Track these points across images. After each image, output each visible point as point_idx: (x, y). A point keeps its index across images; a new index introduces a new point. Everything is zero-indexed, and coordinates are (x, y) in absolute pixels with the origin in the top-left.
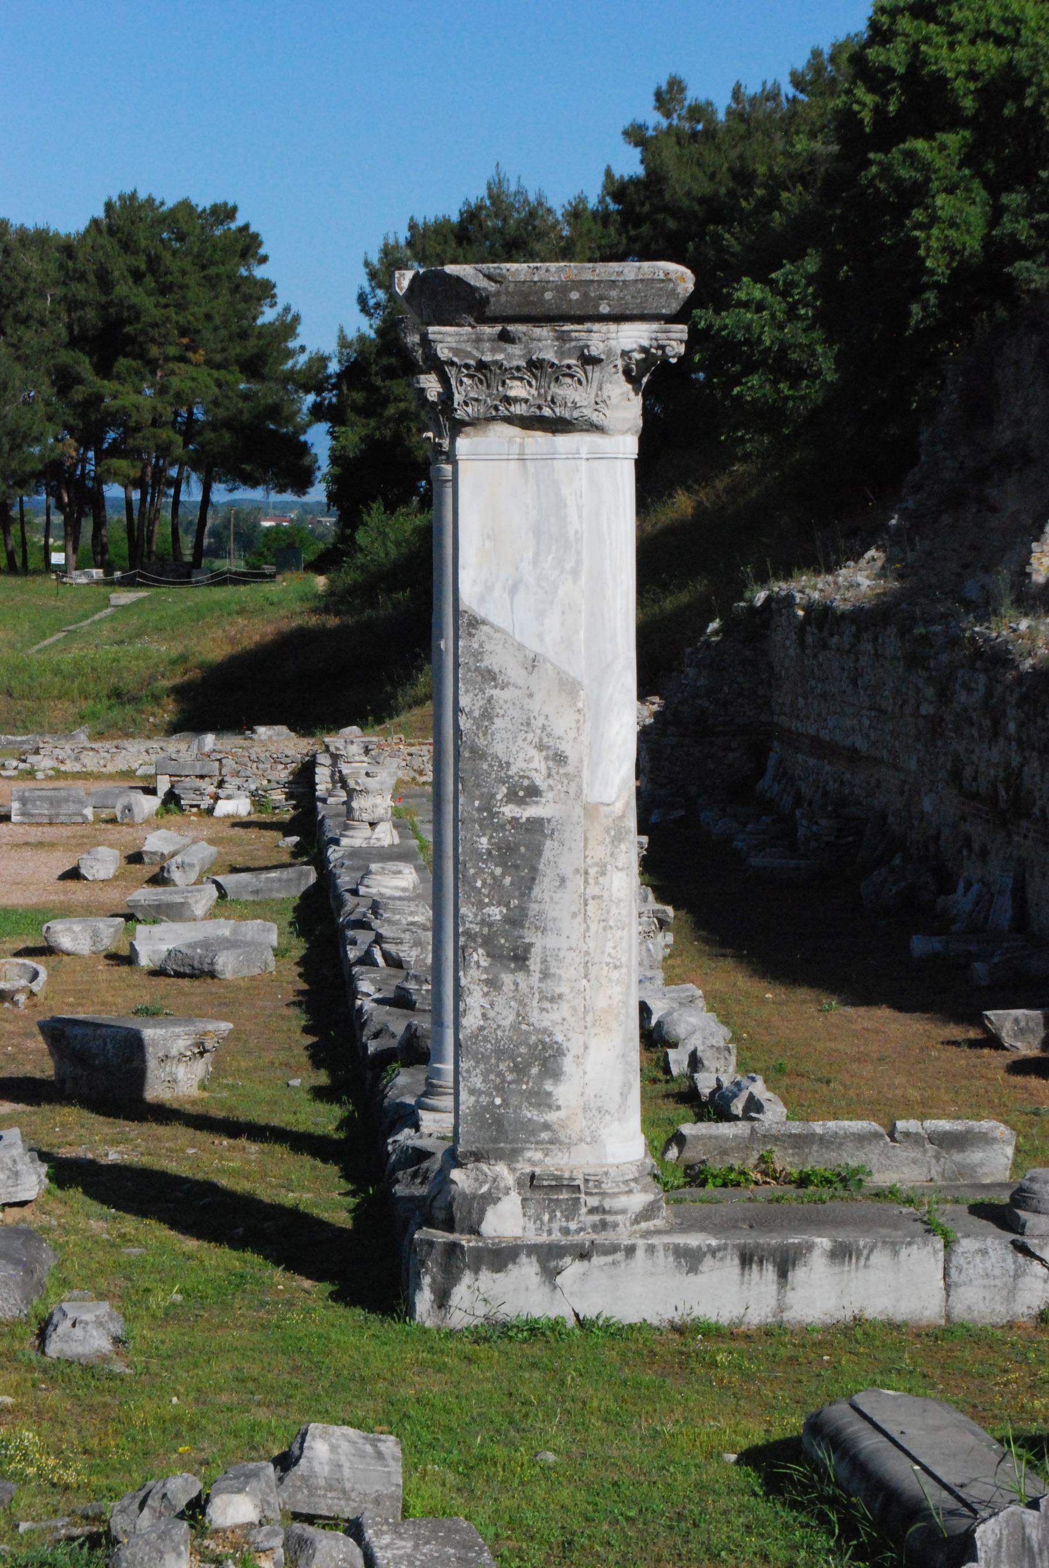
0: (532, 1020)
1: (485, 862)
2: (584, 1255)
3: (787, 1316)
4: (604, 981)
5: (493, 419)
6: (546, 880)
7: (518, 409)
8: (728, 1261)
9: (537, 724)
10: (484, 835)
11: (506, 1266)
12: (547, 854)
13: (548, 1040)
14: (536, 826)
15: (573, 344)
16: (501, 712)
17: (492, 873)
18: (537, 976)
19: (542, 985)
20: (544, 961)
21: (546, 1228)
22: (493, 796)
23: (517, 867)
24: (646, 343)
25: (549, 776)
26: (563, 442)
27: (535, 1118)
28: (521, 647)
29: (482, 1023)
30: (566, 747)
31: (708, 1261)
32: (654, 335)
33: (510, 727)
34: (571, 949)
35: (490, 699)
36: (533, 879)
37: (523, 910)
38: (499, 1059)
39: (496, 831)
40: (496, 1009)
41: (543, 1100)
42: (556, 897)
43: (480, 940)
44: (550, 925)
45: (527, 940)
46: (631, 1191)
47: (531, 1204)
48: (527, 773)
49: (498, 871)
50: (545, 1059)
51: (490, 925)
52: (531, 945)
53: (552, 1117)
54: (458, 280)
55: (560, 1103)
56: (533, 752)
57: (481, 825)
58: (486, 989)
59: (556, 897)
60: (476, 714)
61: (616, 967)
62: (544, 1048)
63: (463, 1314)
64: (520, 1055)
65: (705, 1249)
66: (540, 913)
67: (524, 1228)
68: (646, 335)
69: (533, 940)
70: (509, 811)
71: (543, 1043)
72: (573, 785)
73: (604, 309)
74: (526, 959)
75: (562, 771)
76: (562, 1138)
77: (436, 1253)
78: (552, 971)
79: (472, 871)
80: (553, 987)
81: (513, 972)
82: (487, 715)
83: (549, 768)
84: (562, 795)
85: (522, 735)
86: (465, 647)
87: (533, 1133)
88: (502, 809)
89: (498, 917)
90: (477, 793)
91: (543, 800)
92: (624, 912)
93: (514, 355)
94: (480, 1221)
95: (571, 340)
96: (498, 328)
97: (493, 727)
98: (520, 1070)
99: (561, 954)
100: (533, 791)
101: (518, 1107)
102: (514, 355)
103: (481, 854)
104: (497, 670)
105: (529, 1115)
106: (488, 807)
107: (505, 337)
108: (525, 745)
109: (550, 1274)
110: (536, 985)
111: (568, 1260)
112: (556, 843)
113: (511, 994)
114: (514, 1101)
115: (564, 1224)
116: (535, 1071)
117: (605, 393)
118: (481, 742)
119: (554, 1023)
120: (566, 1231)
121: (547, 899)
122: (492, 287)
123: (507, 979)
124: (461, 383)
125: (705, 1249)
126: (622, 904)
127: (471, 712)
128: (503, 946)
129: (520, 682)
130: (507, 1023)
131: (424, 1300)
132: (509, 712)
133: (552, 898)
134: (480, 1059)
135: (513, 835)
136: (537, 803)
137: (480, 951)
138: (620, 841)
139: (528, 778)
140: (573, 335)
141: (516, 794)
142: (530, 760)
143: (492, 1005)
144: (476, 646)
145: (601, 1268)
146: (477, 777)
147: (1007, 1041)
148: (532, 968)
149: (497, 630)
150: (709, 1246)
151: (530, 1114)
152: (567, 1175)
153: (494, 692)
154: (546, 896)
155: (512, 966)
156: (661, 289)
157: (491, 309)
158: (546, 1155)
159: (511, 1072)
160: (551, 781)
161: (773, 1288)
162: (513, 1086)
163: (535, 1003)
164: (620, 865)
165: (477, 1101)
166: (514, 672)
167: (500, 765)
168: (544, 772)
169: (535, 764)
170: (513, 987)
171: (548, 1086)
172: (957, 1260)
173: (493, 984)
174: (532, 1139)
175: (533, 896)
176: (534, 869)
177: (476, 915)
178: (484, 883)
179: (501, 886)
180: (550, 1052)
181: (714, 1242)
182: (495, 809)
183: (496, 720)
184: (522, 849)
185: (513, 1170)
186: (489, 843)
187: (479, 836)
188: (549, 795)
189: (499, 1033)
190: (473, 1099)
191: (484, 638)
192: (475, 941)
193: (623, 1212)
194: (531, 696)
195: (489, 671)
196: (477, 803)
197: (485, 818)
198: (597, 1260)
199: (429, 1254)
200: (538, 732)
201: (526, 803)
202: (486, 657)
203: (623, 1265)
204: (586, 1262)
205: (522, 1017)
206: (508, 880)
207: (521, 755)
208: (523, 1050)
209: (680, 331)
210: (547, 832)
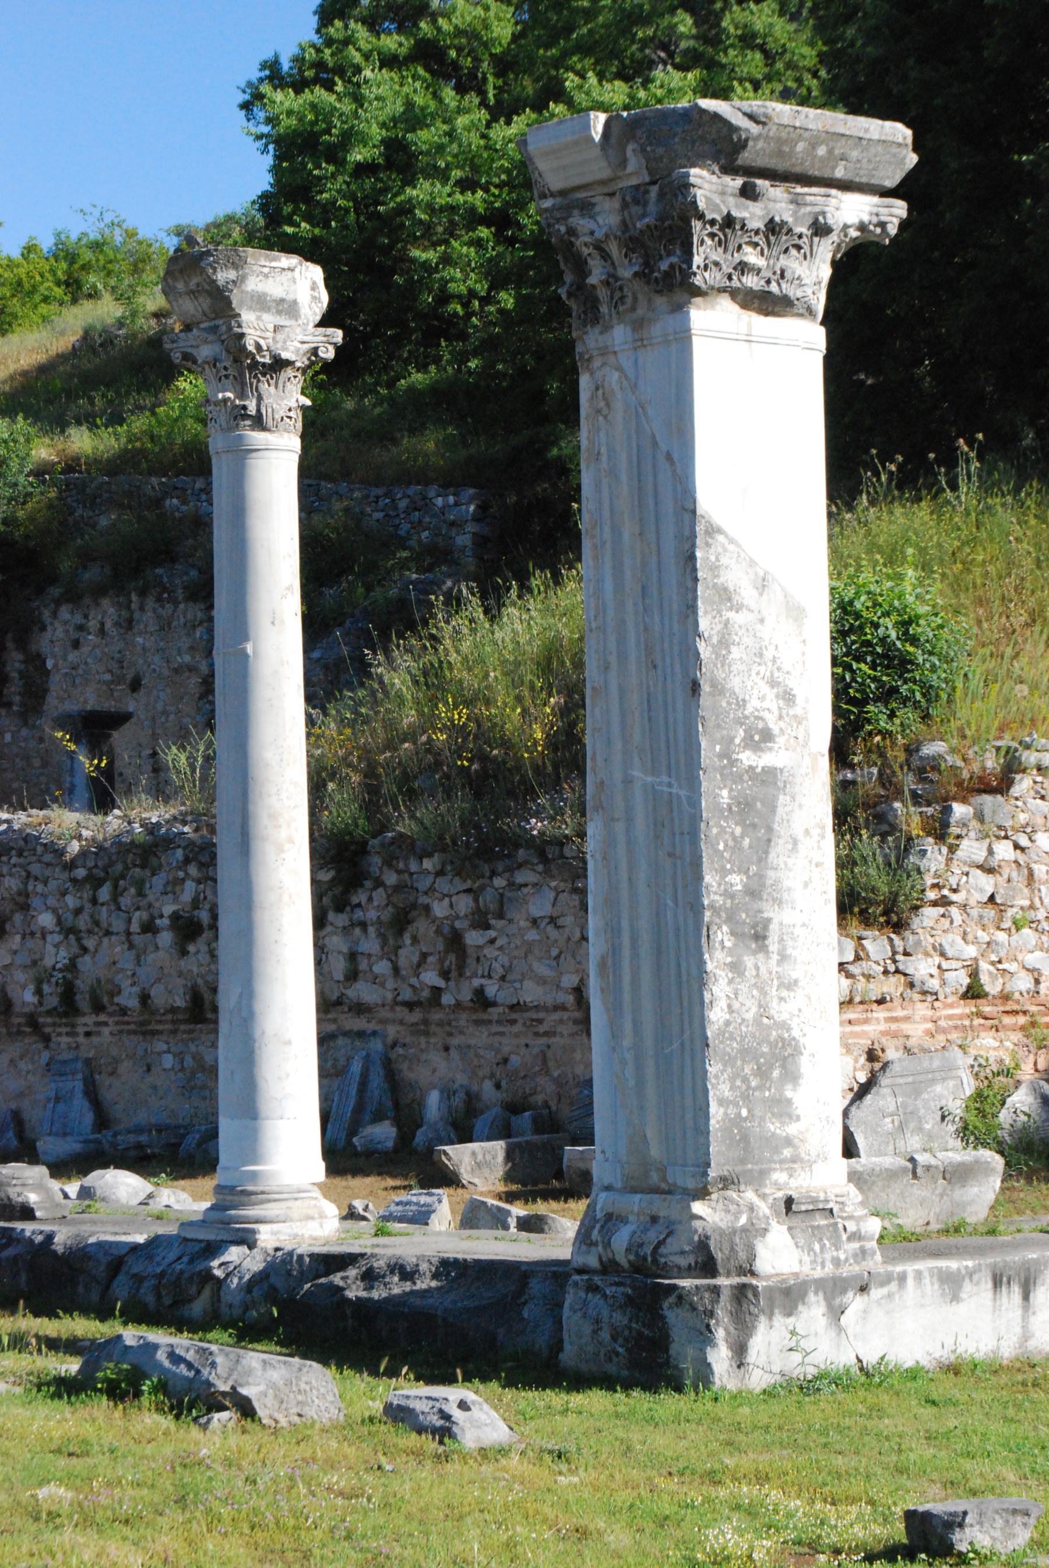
0: (772, 1012)
1: (726, 819)
2: (863, 1289)
3: (1032, 1344)
5: (722, 290)
6: (781, 841)
7: (751, 281)
8: (983, 1286)
9: (768, 654)
10: (725, 787)
11: (796, 1308)
12: (781, 811)
13: (786, 1035)
14: (769, 777)
15: (809, 209)
16: (737, 639)
17: (733, 833)
18: (775, 957)
19: (780, 969)
20: (781, 940)
21: (819, 1260)
22: (731, 740)
23: (754, 826)
24: (866, 218)
25: (781, 717)
27: (778, 1131)
28: (752, 563)
29: (727, 1016)
30: (792, 683)
31: (967, 1287)
32: (875, 210)
33: (744, 657)
34: (804, 925)
35: (727, 623)
36: (769, 841)
37: (760, 877)
38: (743, 1061)
39: (735, 783)
40: (740, 999)
41: (783, 1110)
42: (790, 862)
43: (723, 915)
44: (785, 896)
45: (765, 915)
47: (797, 1232)
48: (762, 714)
49: (738, 830)
50: (785, 1058)
51: (732, 896)
52: (769, 920)
53: (792, 1129)
54: (716, 117)
55: (798, 1112)
56: (765, 689)
57: (722, 775)
58: (730, 975)
59: (790, 862)
60: (715, 640)
62: (783, 1046)
63: (761, 1372)
64: (763, 1055)
65: (963, 1272)
66: (777, 881)
67: (801, 1262)
68: (868, 209)
69: (771, 915)
70: (747, 758)
71: (783, 1039)
72: (801, 728)
73: (839, 173)
74: (765, 938)
75: (791, 712)
76: (803, 1155)
77: (725, 1296)
78: (789, 951)
79: (715, 831)
80: (795, 973)
81: (754, 953)
82: (724, 643)
83: (780, 709)
84: (792, 740)
85: (755, 668)
86: (702, 559)
87: (776, 1150)
88: (741, 756)
89: (739, 887)
90: (718, 735)
91: (776, 746)
93: (753, 214)
94: (752, 1257)
95: (805, 204)
96: (739, 182)
97: (731, 656)
98: (763, 1073)
99: (798, 931)
100: (767, 736)
101: (762, 1119)
102: (753, 214)
103: (722, 810)
104: (732, 589)
105: (772, 1128)
106: (726, 754)
107: (748, 193)
108: (758, 680)
109: (836, 1313)
110: (775, 969)
111: (850, 1294)
112: (788, 798)
113: (753, 981)
114: (758, 1112)
115: (835, 1254)
116: (776, 1073)
118: (720, 674)
119: (792, 1015)
120: (836, 1262)
121: (782, 866)
122: (754, 129)
123: (749, 961)
124: (702, 242)
125: (963, 1272)
127: (710, 637)
128: (744, 922)
129: (753, 605)
130: (749, 1016)
131: (720, 1358)
132: (745, 640)
133: (786, 864)
134: (728, 1061)
135: (750, 788)
136: (770, 749)
137: (725, 928)
139: (762, 719)
140: (809, 198)
141: (752, 737)
142: (762, 699)
143: (736, 994)
144: (713, 558)
145: (878, 1303)
146: (717, 717)
147: (465, 1177)
148: (771, 948)
149: (732, 541)
150: (967, 1267)
151: (773, 1127)
152: (822, 1197)
153: (731, 615)
154: (781, 860)
155: (754, 946)
156: (895, 155)
157: (745, 158)
158: (791, 1176)
159: (755, 1076)
160: (782, 724)
161: (1019, 1312)
162: (757, 1094)
163: (774, 993)
165: (726, 1114)
166: (747, 594)
167: (738, 704)
168: (776, 712)
169: (765, 705)
170: (754, 973)
171: (789, 1094)
173: (736, 968)
174: (776, 1158)
175: (770, 860)
176: (770, 829)
177: (720, 885)
178: (726, 845)
179: (741, 849)
180: (789, 1051)
181: (970, 1263)
182: (735, 756)
183: (733, 649)
184: (759, 804)
185: (763, 1197)
186: (730, 797)
187: (720, 789)
188: (781, 741)
189: (744, 1029)
190: (722, 1110)
191: (720, 550)
192: (720, 917)
194: (762, 621)
195: (725, 589)
196: (718, 748)
197: (725, 767)
198: (876, 1293)
199: (716, 1300)
200: (770, 664)
201: (761, 750)
202: (722, 573)
203: (897, 1296)
204: (866, 1297)
205: (763, 1009)
206: (747, 842)
207: (755, 692)
208: (765, 1049)
209: (900, 209)
210: (780, 784)
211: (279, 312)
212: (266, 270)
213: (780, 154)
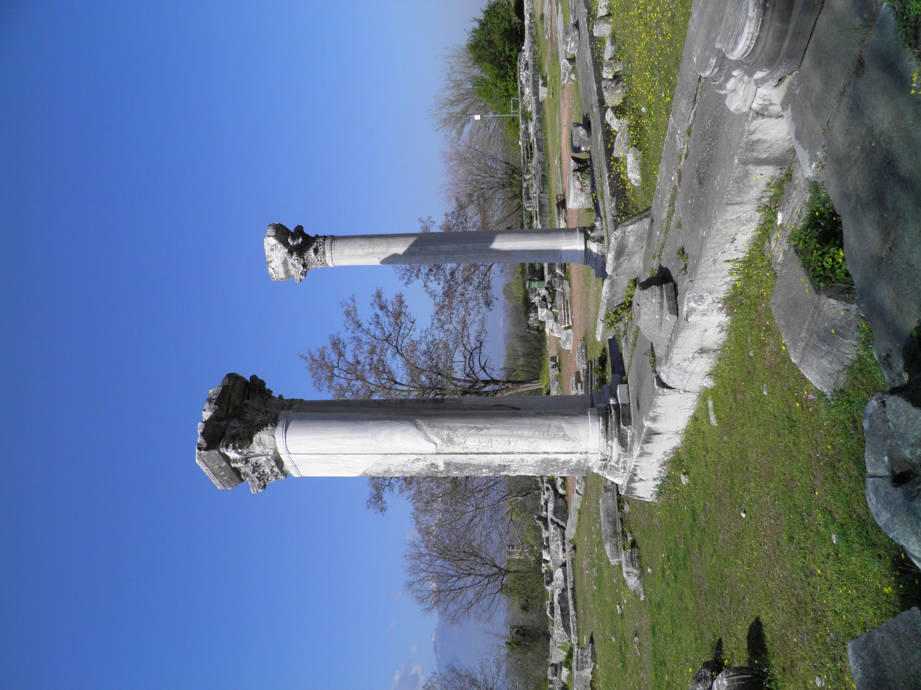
4: (515, 447)
12: (459, 462)
26: (284, 458)
37: (483, 466)
46: (612, 447)
52: (498, 465)
61: (510, 443)
92: (485, 440)
117: (261, 453)
126: (481, 440)
138: (453, 441)
164: (464, 441)
172: (670, 385)
193: (619, 455)
211: (287, 266)
212: (276, 275)
213: (231, 479)
